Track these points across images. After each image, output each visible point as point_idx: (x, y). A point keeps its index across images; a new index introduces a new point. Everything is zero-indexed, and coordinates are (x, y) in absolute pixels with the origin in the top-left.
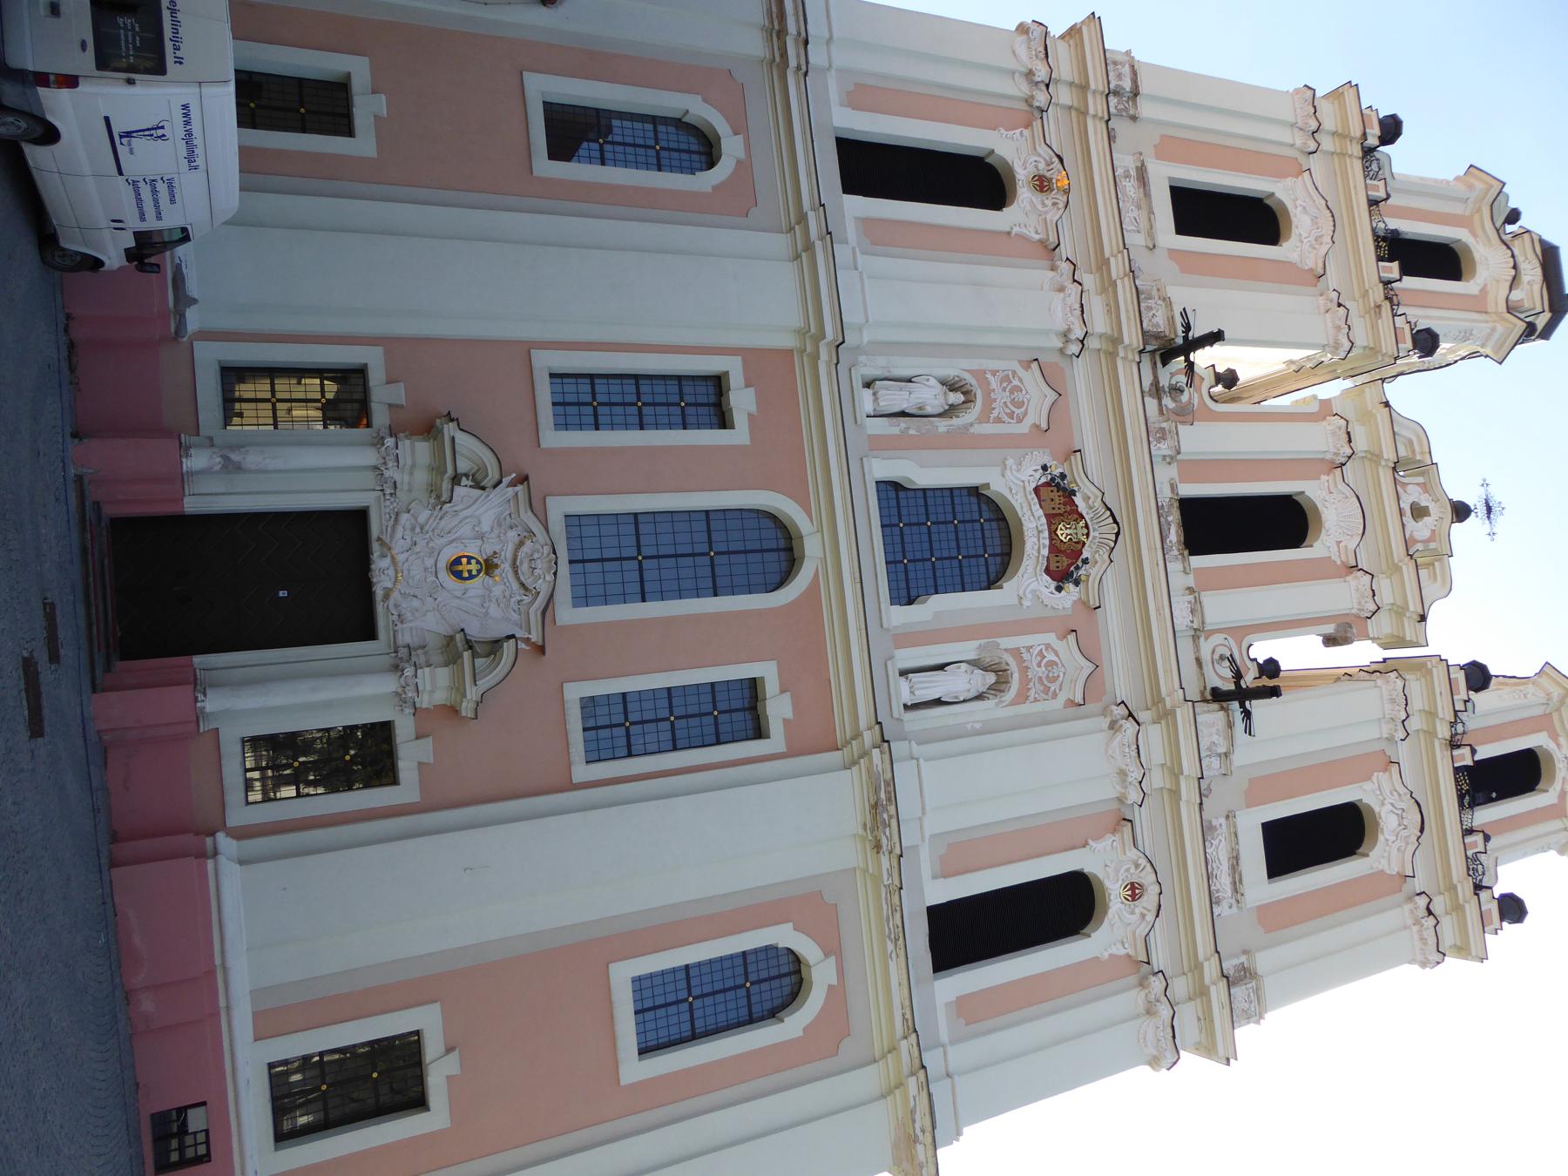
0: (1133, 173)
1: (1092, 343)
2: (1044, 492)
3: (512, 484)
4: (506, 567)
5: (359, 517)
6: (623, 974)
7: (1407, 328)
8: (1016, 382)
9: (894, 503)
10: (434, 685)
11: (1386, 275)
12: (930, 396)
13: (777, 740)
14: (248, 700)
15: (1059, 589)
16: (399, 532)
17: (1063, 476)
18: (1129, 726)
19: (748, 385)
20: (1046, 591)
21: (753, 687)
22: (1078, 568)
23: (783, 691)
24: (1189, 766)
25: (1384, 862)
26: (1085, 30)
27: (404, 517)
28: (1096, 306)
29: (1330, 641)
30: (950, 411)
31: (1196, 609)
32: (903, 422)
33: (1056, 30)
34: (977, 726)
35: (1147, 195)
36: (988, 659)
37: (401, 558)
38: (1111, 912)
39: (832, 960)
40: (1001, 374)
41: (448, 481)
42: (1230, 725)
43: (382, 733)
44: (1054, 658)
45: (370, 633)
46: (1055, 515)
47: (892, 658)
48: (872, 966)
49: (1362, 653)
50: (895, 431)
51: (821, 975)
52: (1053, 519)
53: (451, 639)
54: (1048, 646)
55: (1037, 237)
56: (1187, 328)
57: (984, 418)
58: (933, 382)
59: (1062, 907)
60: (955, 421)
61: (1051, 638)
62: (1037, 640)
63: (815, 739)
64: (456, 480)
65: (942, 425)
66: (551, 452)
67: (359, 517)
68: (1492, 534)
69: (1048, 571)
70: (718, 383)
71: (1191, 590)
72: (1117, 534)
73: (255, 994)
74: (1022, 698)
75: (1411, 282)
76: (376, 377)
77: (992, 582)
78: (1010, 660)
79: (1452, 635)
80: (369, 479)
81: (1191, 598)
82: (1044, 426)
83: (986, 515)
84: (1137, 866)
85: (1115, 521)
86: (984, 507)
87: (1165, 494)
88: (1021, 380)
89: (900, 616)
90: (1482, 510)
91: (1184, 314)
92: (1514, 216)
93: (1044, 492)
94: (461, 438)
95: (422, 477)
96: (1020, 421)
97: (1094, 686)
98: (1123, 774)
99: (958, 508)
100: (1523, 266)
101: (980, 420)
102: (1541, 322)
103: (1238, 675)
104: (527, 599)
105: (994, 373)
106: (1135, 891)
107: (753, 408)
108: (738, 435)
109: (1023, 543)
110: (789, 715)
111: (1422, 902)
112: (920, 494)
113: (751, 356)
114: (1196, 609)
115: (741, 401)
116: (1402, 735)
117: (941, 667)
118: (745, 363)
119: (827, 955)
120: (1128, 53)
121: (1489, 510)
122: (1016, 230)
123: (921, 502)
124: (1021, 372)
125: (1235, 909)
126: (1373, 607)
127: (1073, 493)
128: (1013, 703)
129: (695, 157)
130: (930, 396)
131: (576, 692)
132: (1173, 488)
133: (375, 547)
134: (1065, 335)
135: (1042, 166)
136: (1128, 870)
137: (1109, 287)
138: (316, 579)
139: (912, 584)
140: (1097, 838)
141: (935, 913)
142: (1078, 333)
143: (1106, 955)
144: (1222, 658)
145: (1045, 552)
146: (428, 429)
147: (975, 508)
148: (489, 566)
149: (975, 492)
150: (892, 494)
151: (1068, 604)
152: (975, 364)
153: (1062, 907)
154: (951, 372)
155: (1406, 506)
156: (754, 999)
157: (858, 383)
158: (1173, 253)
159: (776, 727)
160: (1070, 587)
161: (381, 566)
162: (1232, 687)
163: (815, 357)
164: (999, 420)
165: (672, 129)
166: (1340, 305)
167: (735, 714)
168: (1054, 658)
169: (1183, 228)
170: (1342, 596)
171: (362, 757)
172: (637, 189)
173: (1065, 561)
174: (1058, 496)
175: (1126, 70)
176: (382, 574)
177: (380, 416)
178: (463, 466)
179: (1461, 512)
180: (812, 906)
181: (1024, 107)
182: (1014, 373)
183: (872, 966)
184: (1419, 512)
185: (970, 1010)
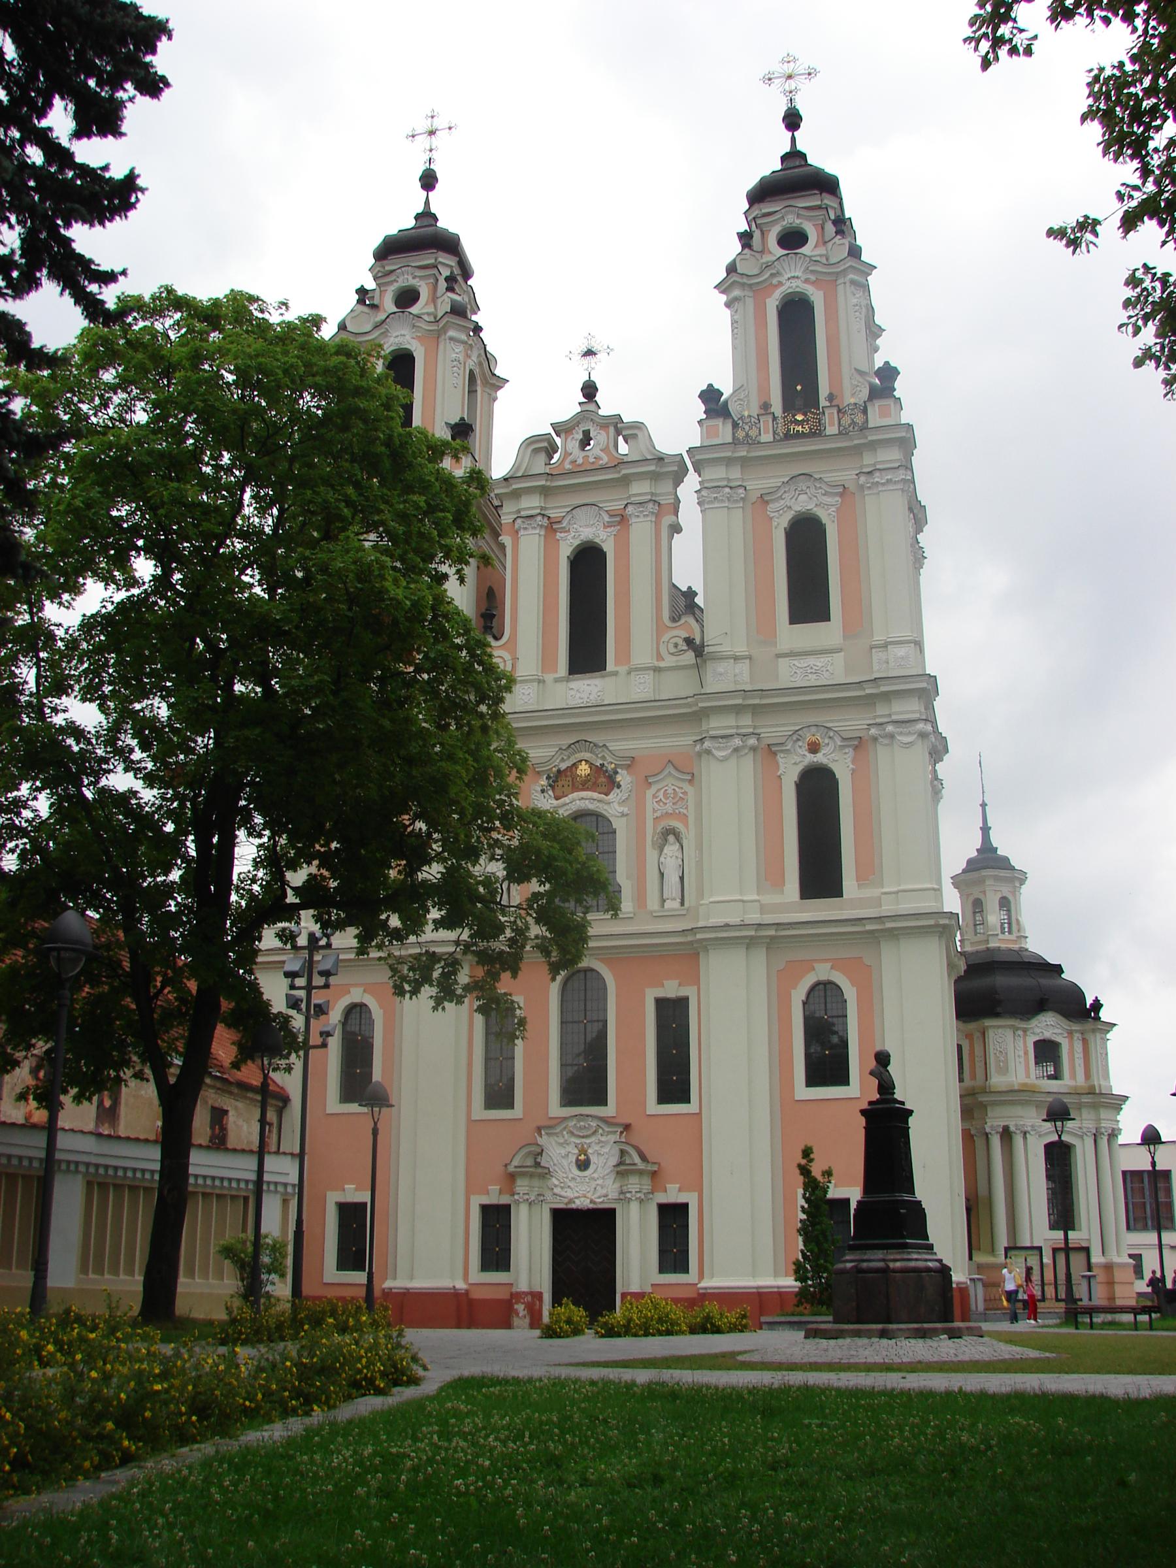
2: (559, 792)
3: (541, 1135)
4: (583, 1140)
15: (619, 786)
16: (563, 1193)
17: (548, 778)
18: (707, 744)
21: (660, 1003)
23: (663, 986)
27: (557, 1190)
37: (576, 1195)
38: (825, 761)
39: (816, 965)
41: (538, 1169)
43: (664, 1209)
45: (614, 1210)
46: (573, 785)
47: (651, 912)
51: (823, 972)
52: (575, 789)
53: (618, 1173)
54: (654, 796)
59: (817, 796)
61: (650, 793)
62: (650, 804)
64: (537, 1164)
66: (524, 1114)
73: (776, 1274)
74: (684, 818)
76: (486, 1201)
79: (676, 428)
80: (536, 1209)
92: (362, 292)
93: (559, 792)
94: (515, 1162)
95: (536, 1182)
104: (600, 1131)
111: (863, 479)
116: (741, 491)
117: (662, 875)
121: (589, 353)
127: (559, 771)
131: (653, 1107)
133: (570, 1206)
138: (584, 1237)
145: (595, 795)
146: (512, 1177)
148: (583, 1151)
151: (628, 779)
153: (817, 796)
159: (682, 992)
161: (579, 1204)
170: (641, 529)
171: (673, 1219)
177: (504, 1200)
178: (530, 1162)
179: (590, 391)
184: (586, 440)
185: (869, 872)
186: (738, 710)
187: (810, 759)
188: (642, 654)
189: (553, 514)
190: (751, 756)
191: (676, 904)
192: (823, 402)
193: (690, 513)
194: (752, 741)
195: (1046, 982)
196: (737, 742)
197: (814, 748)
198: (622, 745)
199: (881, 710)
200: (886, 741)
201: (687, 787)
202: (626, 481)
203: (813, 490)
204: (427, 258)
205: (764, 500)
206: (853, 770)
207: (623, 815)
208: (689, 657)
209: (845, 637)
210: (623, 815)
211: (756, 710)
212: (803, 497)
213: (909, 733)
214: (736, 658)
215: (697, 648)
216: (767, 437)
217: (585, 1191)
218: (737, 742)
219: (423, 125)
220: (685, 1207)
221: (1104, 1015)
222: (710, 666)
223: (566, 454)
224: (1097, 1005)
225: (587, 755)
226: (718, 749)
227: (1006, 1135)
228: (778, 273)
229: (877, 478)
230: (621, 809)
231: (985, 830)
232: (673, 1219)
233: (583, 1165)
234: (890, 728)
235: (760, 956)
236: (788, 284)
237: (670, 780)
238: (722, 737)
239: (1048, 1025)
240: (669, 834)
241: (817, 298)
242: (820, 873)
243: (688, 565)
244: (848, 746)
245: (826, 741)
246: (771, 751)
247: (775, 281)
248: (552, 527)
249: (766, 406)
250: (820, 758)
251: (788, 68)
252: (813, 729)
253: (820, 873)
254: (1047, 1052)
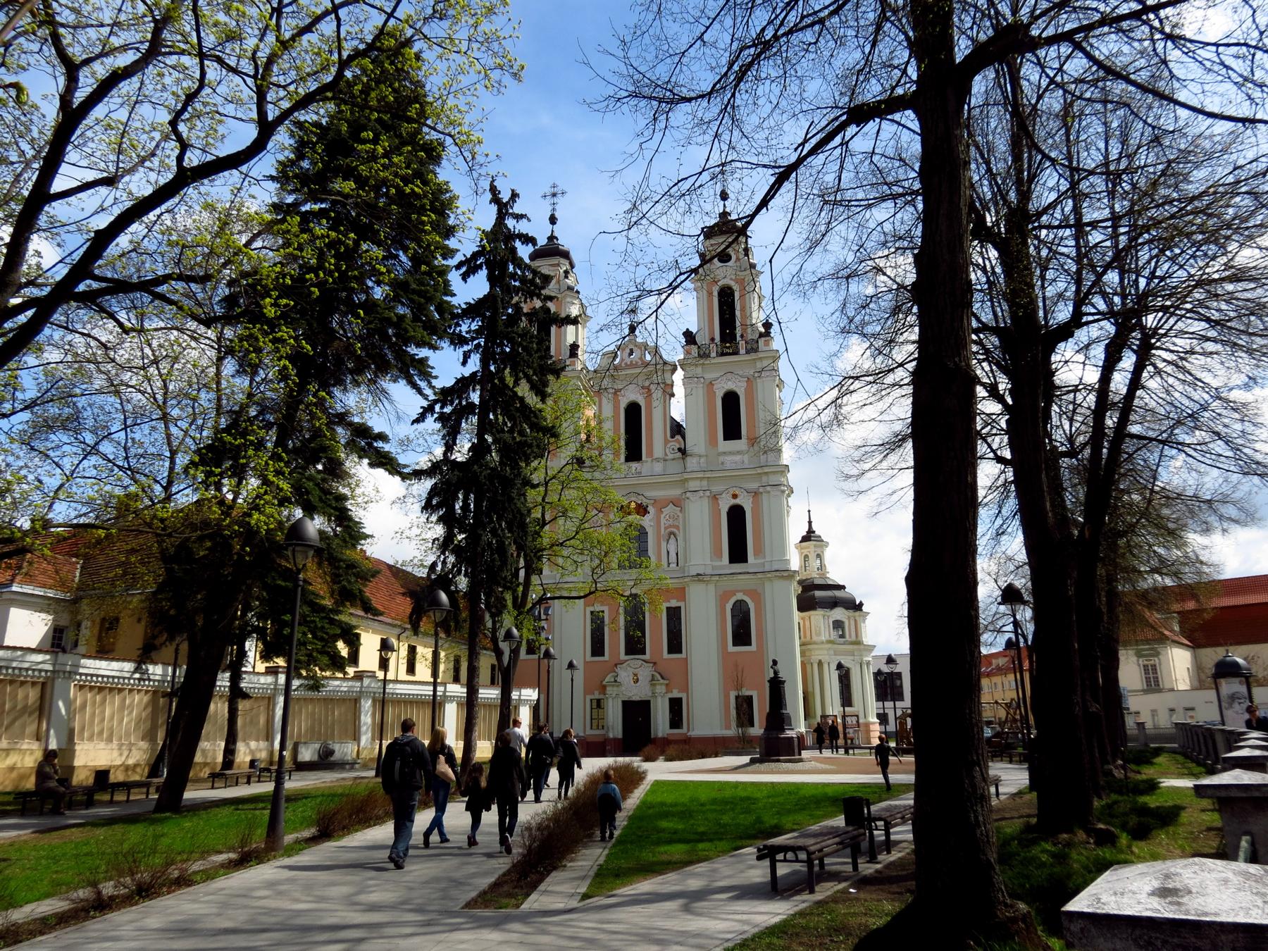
5: (624, 703)
6: (731, 648)
10: (660, 689)
14: (660, 728)
24: (700, 475)
43: (671, 700)
45: (648, 702)
48: (740, 582)
51: (740, 596)
63: (681, 593)
67: (624, 703)
79: (673, 351)
97: (677, 503)
106: (735, 496)
108: (606, 609)
114: (657, 460)
138: (637, 712)
146: (604, 687)
161: (634, 699)
167: (674, 615)
170: (657, 394)
171: (676, 706)
176: (638, 698)
177: (601, 696)
180: (723, 598)
183: (740, 582)
184: (631, 352)
185: (759, 551)
188: (658, 451)
192: (738, 338)
193: (679, 389)
195: (838, 593)
197: (735, 496)
199: (764, 479)
204: (554, 260)
208: (679, 455)
215: (683, 451)
216: (714, 354)
217: (637, 693)
218: (701, 493)
219: (549, 191)
220: (681, 699)
221: (864, 608)
222: (688, 459)
223: (622, 360)
224: (861, 604)
227: (820, 663)
231: (810, 522)
232: (676, 706)
233: (637, 681)
234: (768, 488)
239: (839, 613)
241: (736, 287)
242: (738, 552)
243: (678, 410)
249: (713, 340)
250: (737, 501)
253: (738, 552)
254: (838, 625)
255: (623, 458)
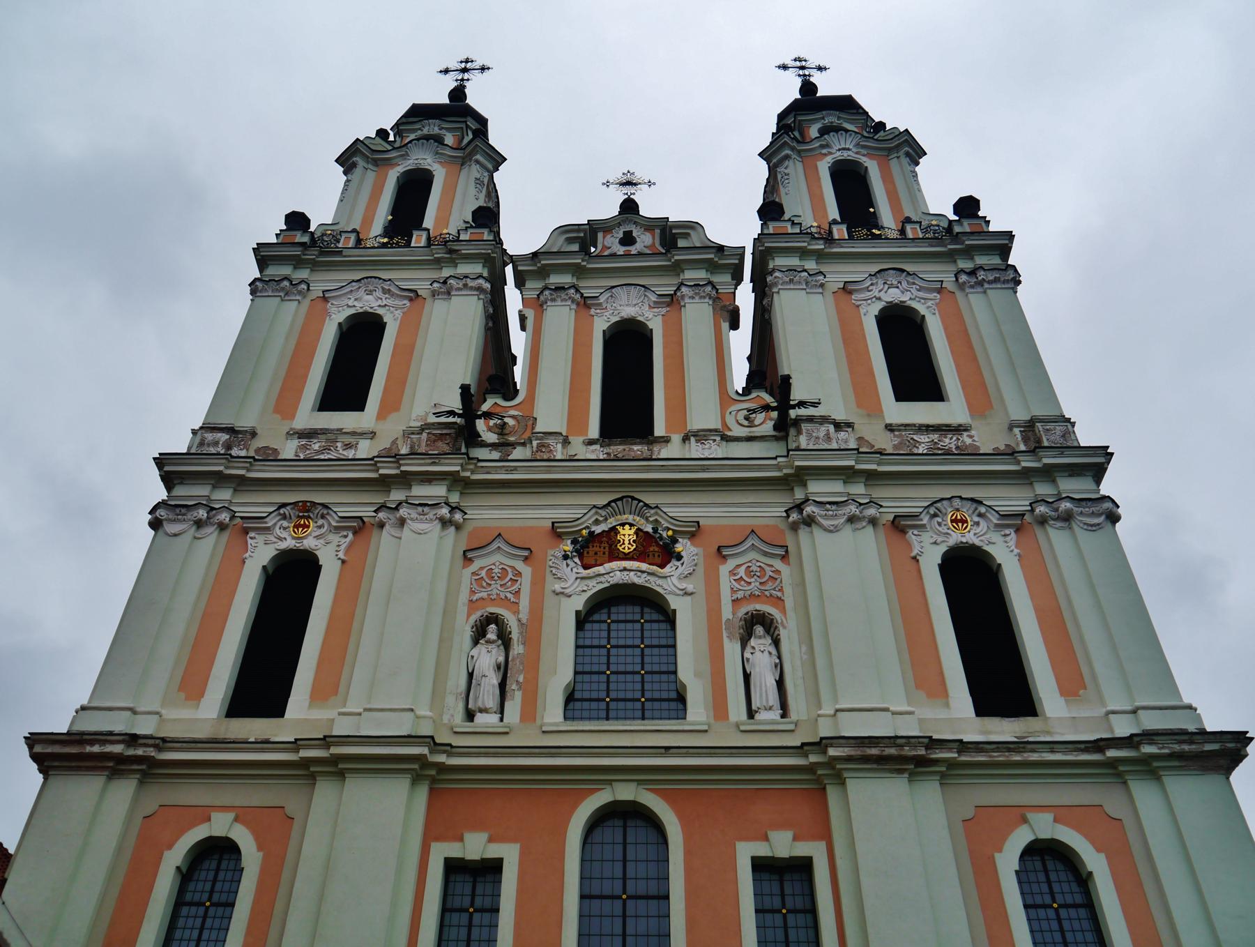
0: (304, 442)
1: (454, 498)
7: (470, 231)
8: (483, 573)
9: (586, 705)
11: (423, 242)
12: (487, 658)
13: (814, 849)
15: (679, 557)
17: (574, 542)
18: (809, 509)
19: (461, 839)
20: (681, 569)
21: (760, 865)
22: (661, 538)
25: (930, 303)
26: (167, 468)
28: (420, 491)
29: (735, 325)
30: (505, 639)
31: (701, 436)
32: (512, 686)
33: (161, 493)
34: (804, 648)
35: (324, 432)
36: (738, 632)
38: (977, 542)
40: (475, 585)
42: (811, 419)
44: (743, 568)
47: (737, 725)
49: (745, 297)
50: (518, 695)
52: (615, 555)
54: (732, 573)
55: (351, 535)
56: (451, 413)
57: (514, 606)
58: (474, 652)
60: (515, 636)
61: (724, 569)
62: (725, 583)
65: (517, 649)
68: (650, 184)
69: (662, 566)
70: (453, 867)
71: (686, 439)
72: (633, 498)
74: (779, 601)
75: (428, 222)
77: (669, 618)
78: (742, 611)
81: (692, 439)
82: (526, 553)
83: (604, 617)
84: (935, 515)
85: (621, 499)
86: (596, 617)
87: (597, 452)
88: (482, 568)
89: (697, 711)
90: (629, 190)
91: (438, 414)
96: (519, 574)
98: (851, 519)
99: (596, 642)
100: (425, 131)
101: (517, 612)
102: (473, 125)
103: (766, 408)
105: (473, 592)
107: (484, 836)
108: (510, 854)
109: (634, 585)
110: (789, 835)
111: (963, 278)
112: (579, 678)
113: (431, 835)
114: (701, 436)
115: (475, 847)
117: (747, 677)
118: (438, 839)
119: (1025, 820)
120: (194, 432)
121: (629, 183)
122: (341, 555)
123: (586, 678)
124: (475, 566)
125: (973, 433)
126: (709, 288)
127: (592, 533)
128: (784, 611)
129: (224, 864)
130: (487, 658)
132: (591, 442)
134: (445, 523)
135: (285, 524)
136: (939, 524)
137: (405, 480)
139: (665, 695)
140: (909, 546)
141: (983, 708)
142: (445, 511)
143: (1016, 551)
144: (747, 418)
145: (644, 566)
147: (596, 626)
149: (582, 621)
150: (578, 705)
151: (694, 550)
152: (462, 609)
154: (468, 633)
155: (621, 250)
156: (1069, 900)
157: (468, 727)
158: (382, 415)
160: (678, 548)
162: (775, 414)
163: (442, 768)
164: (517, 593)
165: (191, 886)
166: (445, 282)
168: (743, 568)
169: (360, 406)
172: (249, 932)
173: (654, 548)
174: (592, 547)
175: (210, 436)
179: (629, 207)
181: (226, 534)
182: (473, 574)
184: (628, 240)
186: (848, 474)
187: (956, 538)
189: (587, 293)
190: (870, 529)
191: (775, 715)
194: (872, 511)
196: (853, 509)
198: (677, 509)
200: (1059, 524)
201: (778, 564)
202: (677, 268)
203: (904, 284)
205: (847, 289)
206: (1019, 555)
207: (687, 594)
209: (972, 415)
210: (687, 594)
211: (871, 477)
212: (892, 291)
213: (1093, 514)
214: (838, 426)
219: (454, 65)
225: (630, 518)
226: (826, 517)
228: (827, 146)
229: (981, 275)
230: (683, 585)
235: (930, 792)
236: (839, 153)
237: (753, 555)
238: (830, 503)
240: (756, 624)
244: (1008, 526)
245: (976, 519)
246: (900, 526)
247: (824, 151)
248: (585, 304)
250: (970, 536)
251: (798, 64)
252: (957, 503)
255: (594, 431)
